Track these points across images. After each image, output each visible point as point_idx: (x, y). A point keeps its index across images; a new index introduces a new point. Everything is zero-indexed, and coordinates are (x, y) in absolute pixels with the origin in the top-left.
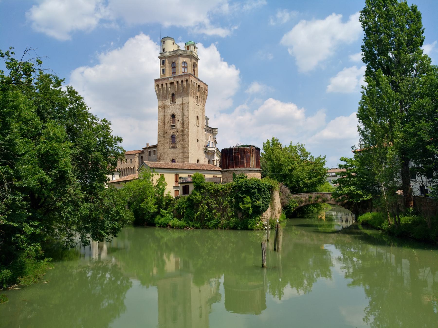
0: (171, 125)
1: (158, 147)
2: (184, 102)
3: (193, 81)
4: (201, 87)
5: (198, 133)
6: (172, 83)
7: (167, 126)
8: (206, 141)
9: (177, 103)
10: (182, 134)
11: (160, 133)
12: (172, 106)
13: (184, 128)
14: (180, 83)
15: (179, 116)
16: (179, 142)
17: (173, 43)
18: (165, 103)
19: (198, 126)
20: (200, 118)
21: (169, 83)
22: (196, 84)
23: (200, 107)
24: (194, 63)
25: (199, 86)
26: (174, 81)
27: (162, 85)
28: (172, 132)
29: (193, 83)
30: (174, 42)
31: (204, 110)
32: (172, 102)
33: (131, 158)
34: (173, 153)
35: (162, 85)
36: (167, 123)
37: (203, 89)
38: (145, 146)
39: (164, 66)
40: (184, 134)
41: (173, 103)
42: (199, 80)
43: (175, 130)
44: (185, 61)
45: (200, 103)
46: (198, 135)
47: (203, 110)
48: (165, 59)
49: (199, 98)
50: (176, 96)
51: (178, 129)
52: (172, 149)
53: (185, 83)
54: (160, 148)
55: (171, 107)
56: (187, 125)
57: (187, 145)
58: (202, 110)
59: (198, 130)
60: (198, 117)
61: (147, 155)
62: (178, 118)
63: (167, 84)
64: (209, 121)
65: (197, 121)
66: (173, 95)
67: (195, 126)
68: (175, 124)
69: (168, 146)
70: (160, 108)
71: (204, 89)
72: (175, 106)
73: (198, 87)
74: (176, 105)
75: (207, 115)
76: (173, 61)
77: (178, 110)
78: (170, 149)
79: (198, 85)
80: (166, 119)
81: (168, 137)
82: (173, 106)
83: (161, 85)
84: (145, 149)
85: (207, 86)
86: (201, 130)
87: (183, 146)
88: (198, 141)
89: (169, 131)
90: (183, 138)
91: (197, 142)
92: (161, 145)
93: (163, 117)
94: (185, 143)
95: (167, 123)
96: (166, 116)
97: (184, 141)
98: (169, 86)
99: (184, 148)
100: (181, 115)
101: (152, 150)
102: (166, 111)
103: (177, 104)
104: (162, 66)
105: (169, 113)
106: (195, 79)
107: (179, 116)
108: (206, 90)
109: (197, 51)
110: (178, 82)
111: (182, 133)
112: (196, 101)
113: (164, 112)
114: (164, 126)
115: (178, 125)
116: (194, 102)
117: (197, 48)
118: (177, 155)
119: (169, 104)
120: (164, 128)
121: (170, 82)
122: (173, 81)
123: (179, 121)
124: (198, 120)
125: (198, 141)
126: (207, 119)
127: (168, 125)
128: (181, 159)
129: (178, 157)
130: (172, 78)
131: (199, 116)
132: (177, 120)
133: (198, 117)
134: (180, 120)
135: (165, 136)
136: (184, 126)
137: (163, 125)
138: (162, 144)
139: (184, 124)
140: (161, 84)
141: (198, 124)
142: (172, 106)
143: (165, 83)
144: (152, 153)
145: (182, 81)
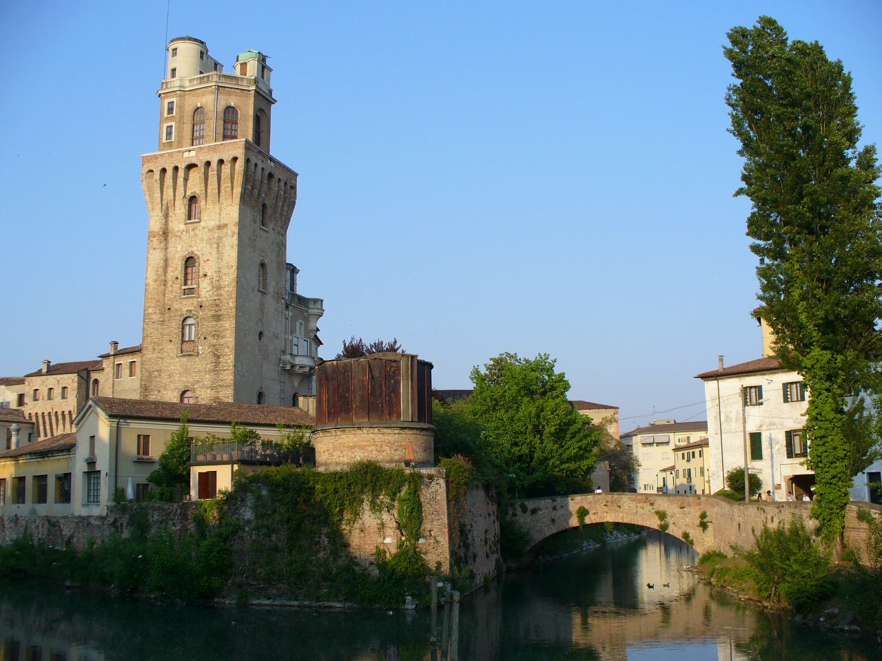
0: (184, 287)
1: (144, 351)
2: (223, 222)
3: (254, 160)
4: (277, 177)
6: (191, 167)
7: (172, 291)
8: (287, 337)
9: (202, 224)
11: (150, 311)
12: (187, 231)
14: (214, 165)
15: (208, 260)
16: (205, 338)
17: (202, 53)
19: (263, 293)
20: (271, 268)
21: (182, 166)
22: (263, 169)
24: (261, 110)
25: (271, 176)
26: (200, 160)
27: (164, 171)
28: (186, 306)
29: (253, 167)
30: (204, 51)
33: (64, 385)
34: (187, 371)
37: (282, 184)
38: (109, 350)
39: (171, 119)
40: (220, 315)
41: (191, 223)
42: (272, 159)
44: (232, 104)
45: (271, 226)
46: (261, 320)
47: (281, 246)
48: (175, 100)
49: (269, 211)
50: (202, 203)
51: (204, 299)
52: (185, 359)
53: (226, 169)
54: (148, 355)
55: (185, 236)
56: (231, 289)
59: (262, 304)
60: (263, 265)
61: (111, 376)
62: (207, 266)
63: (176, 169)
64: (299, 277)
65: (261, 278)
66: (193, 199)
67: (253, 290)
68: (195, 286)
69: (172, 349)
70: (154, 237)
71: (286, 184)
72: (197, 232)
73: (266, 177)
75: (290, 259)
76: (199, 105)
77: (204, 244)
78: (177, 360)
79: (266, 173)
80: (170, 269)
81: (175, 325)
82: (192, 233)
83: (159, 173)
84: (107, 356)
85: (296, 175)
86: (270, 301)
87: (217, 350)
88: (261, 334)
89: (176, 306)
91: (260, 338)
92: (150, 347)
93: (161, 263)
94: (222, 341)
95: (170, 283)
96: (170, 262)
97: (218, 336)
98: (181, 173)
101: (125, 361)
102: (171, 245)
103: (204, 228)
104: (167, 118)
105: (178, 252)
106: (260, 157)
107: (208, 260)
108: (292, 187)
109: (269, 80)
110: (208, 164)
111: (213, 313)
112: (259, 218)
113: (166, 249)
115: (205, 288)
116: (255, 222)
117: (270, 70)
118: (197, 378)
119: (182, 227)
120: (164, 295)
121: (188, 163)
122: (194, 161)
124: (265, 274)
125: (261, 334)
126: (294, 270)
127: (176, 287)
128: (209, 391)
129: (201, 384)
130: (193, 153)
131: (266, 261)
132: (201, 274)
133: (263, 265)
134: (208, 274)
138: (154, 343)
140: (160, 168)
141: (265, 286)
143: (173, 165)
144: (125, 371)
145: (221, 162)
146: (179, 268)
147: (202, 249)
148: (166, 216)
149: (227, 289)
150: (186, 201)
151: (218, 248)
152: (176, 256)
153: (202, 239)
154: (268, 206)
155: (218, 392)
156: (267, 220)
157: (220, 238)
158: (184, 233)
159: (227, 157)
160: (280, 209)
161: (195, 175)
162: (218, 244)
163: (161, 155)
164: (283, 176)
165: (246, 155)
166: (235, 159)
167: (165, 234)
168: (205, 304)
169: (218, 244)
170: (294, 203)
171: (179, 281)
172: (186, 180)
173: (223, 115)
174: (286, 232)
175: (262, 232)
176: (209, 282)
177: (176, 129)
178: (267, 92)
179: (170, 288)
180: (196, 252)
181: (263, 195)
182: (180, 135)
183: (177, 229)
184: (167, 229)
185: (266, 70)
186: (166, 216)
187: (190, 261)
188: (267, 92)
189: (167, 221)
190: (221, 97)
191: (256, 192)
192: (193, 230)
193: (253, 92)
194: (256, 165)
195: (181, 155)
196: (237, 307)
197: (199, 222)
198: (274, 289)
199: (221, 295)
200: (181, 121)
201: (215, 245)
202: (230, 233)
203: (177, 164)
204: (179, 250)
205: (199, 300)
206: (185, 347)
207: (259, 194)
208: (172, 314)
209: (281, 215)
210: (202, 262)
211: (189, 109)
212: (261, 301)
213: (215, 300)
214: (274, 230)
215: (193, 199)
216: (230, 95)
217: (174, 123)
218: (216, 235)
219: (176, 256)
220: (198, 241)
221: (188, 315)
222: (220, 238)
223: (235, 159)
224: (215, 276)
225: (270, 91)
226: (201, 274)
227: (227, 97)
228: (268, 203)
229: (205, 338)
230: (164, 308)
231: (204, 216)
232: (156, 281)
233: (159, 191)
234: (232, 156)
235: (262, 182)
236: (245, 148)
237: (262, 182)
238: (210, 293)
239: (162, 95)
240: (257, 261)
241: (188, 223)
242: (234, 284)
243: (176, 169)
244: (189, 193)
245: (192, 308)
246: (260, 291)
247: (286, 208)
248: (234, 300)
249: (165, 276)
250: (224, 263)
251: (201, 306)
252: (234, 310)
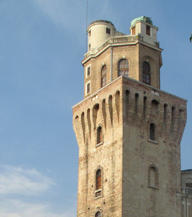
0: (96, 192)
5: (154, 204)
9: (105, 145)
10: (110, 208)
11: (80, 212)
15: (108, 169)
17: (108, 31)
19: (154, 188)
21: (91, 107)
22: (145, 98)
23: (163, 147)
27: (83, 114)
28: (96, 205)
30: (110, 27)
31: (176, 153)
32: (97, 145)
36: (89, 190)
37: (169, 108)
40: (114, 207)
43: (101, 200)
44: (124, 57)
45: (161, 140)
46: (152, 208)
49: (157, 129)
50: (103, 129)
51: (106, 198)
55: (95, 157)
56: (119, 187)
58: (170, 153)
67: (142, 186)
71: (173, 108)
72: (102, 151)
74: (104, 148)
79: (149, 100)
80: (89, 181)
86: (163, 195)
102: (89, 164)
103: (105, 147)
107: (108, 169)
111: (110, 206)
113: (87, 167)
119: (95, 150)
123: (108, 181)
131: (157, 165)
132: (104, 180)
133: (153, 168)
134: (108, 179)
136: (115, 190)
140: (81, 113)
141: (157, 183)
142: (97, 152)
145: (111, 97)
146: (93, 179)
147: (105, 163)
148: (87, 145)
149: (117, 187)
150: (96, 131)
151: (112, 159)
152: (92, 171)
153: (104, 156)
154: (156, 125)
156: (156, 136)
157: (113, 152)
158: (96, 154)
159: (113, 93)
160: (169, 127)
161: (100, 112)
162: (112, 156)
163: (81, 104)
164: (170, 104)
165: (123, 87)
167: (87, 157)
168: (107, 201)
169: (112, 156)
170: (184, 123)
171: (93, 188)
172: (95, 117)
173: (117, 66)
174: (180, 143)
175: (150, 144)
176: (108, 184)
177: (91, 85)
178: (153, 44)
179: (89, 194)
180: (101, 166)
181: (148, 117)
182: (94, 88)
183: (92, 152)
184: (87, 154)
185: (151, 29)
186: (87, 145)
187: (98, 172)
188: (153, 44)
189: (87, 148)
190: (115, 53)
191: (140, 115)
192: (100, 150)
193: (138, 45)
194: (137, 95)
195: (91, 99)
196: (123, 200)
197: (103, 144)
198: (167, 185)
199: (115, 192)
200: (94, 78)
201: (111, 158)
202: (118, 147)
203: (89, 107)
204: (93, 166)
205: (104, 198)
207: (144, 116)
208: (90, 212)
209: (172, 131)
210: (104, 171)
211: (99, 69)
212: (152, 194)
213: (111, 197)
214: (165, 142)
215: (100, 129)
216: (122, 50)
217: (90, 81)
218: (111, 150)
219: (92, 171)
220: (102, 158)
221: (98, 210)
222: (113, 152)
223: (118, 93)
224: (111, 179)
225: (157, 44)
226: (104, 180)
227: (119, 53)
228: (156, 122)
231: (105, 139)
232: (82, 191)
233: (82, 129)
234: (116, 91)
235: (145, 108)
236: (123, 83)
237: (145, 108)
238: (109, 193)
239: (85, 65)
240: (147, 164)
242: (121, 183)
244: (97, 126)
245: (100, 206)
246: (150, 187)
247: (176, 126)
248: (121, 194)
249: (87, 186)
250: (115, 170)
251: (104, 203)
252: (121, 202)
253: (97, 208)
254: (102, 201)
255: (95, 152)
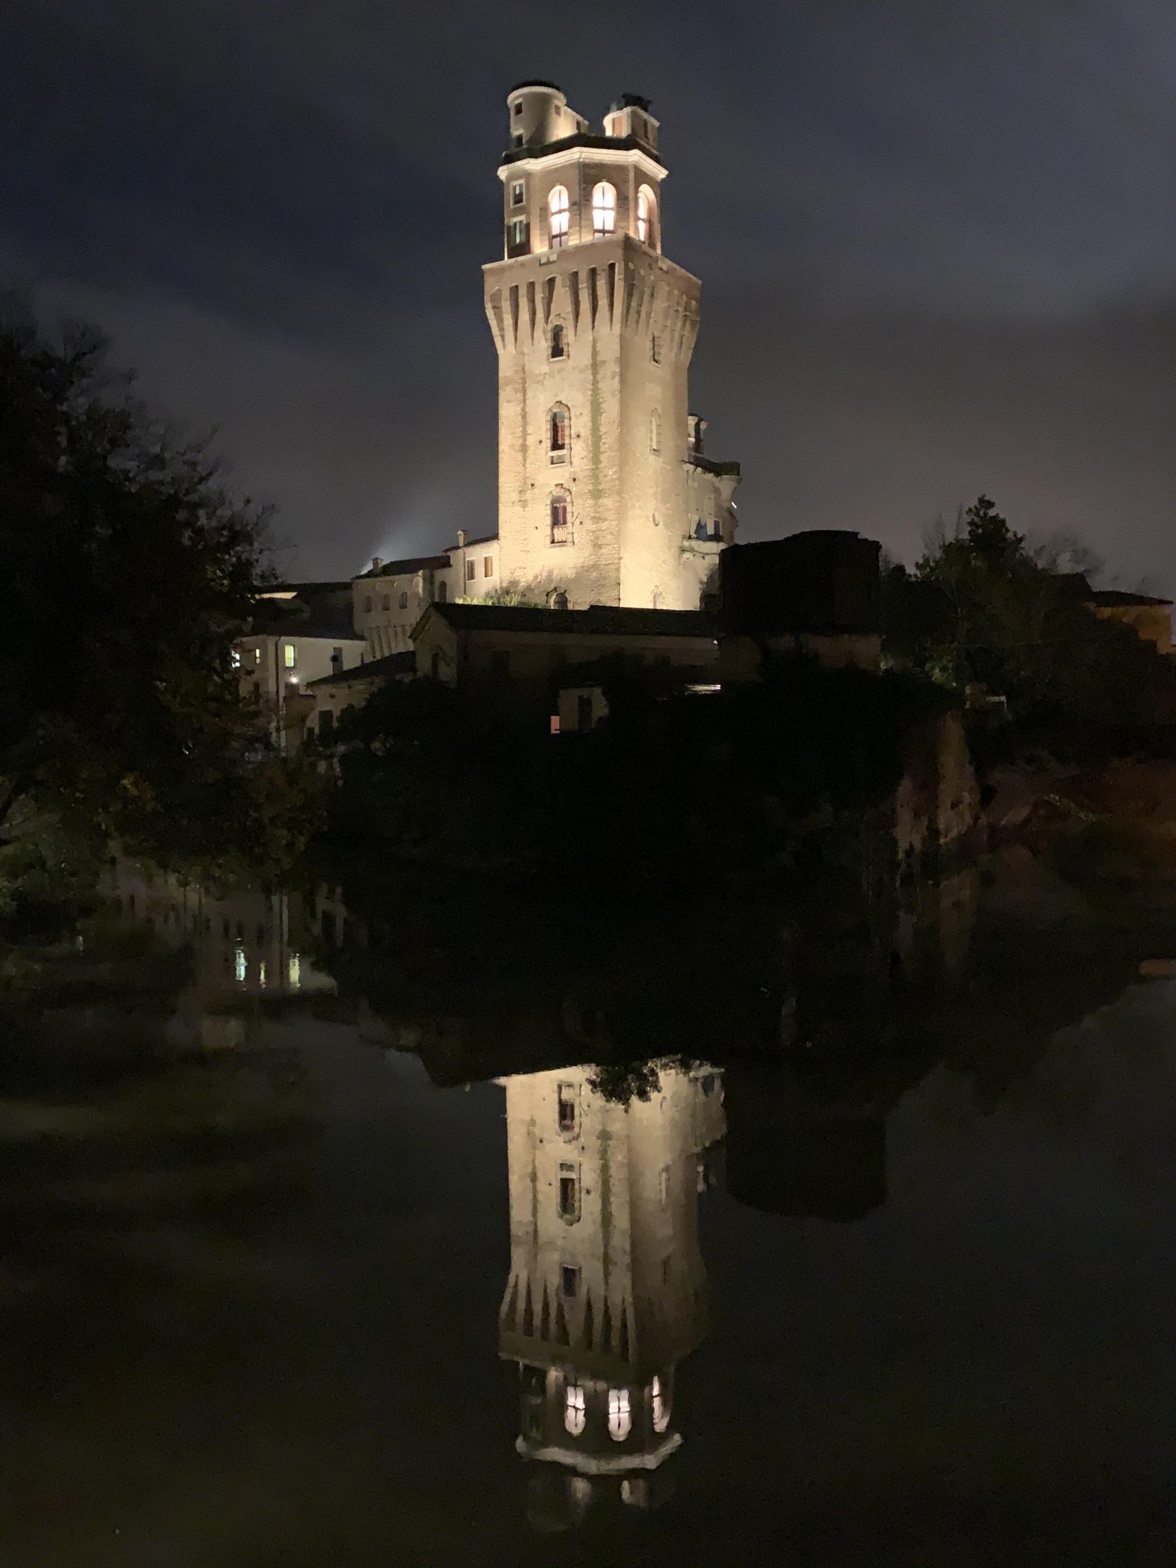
13: (602, 465)
14: (583, 276)
15: (581, 414)
18: (526, 362)
27: (515, 290)
35: (515, 290)
40: (601, 491)
51: (579, 470)
57: (612, 533)
90: (596, 504)
99: (600, 547)
100: (587, 411)
102: (529, 394)
111: (591, 487)
113: (524, 401)
114: (525, 460)
119: (545, 368)
123: (581, 439)
134: (582, 435)
135: (525, 501)
137: (520, 458)
139: (602, 450)
155: (600, 594)
158: (547, 377)
166: (612, 266)
202: (609, 374)
206: (560, 534)
208: (536, 491)
229: (581, 523)
230: (525, 483)
241: (551, 362)
243: (532, 285)
251: (574, 480)
253: (557, 485)
254: (567, 475)
255: (546, 373)
